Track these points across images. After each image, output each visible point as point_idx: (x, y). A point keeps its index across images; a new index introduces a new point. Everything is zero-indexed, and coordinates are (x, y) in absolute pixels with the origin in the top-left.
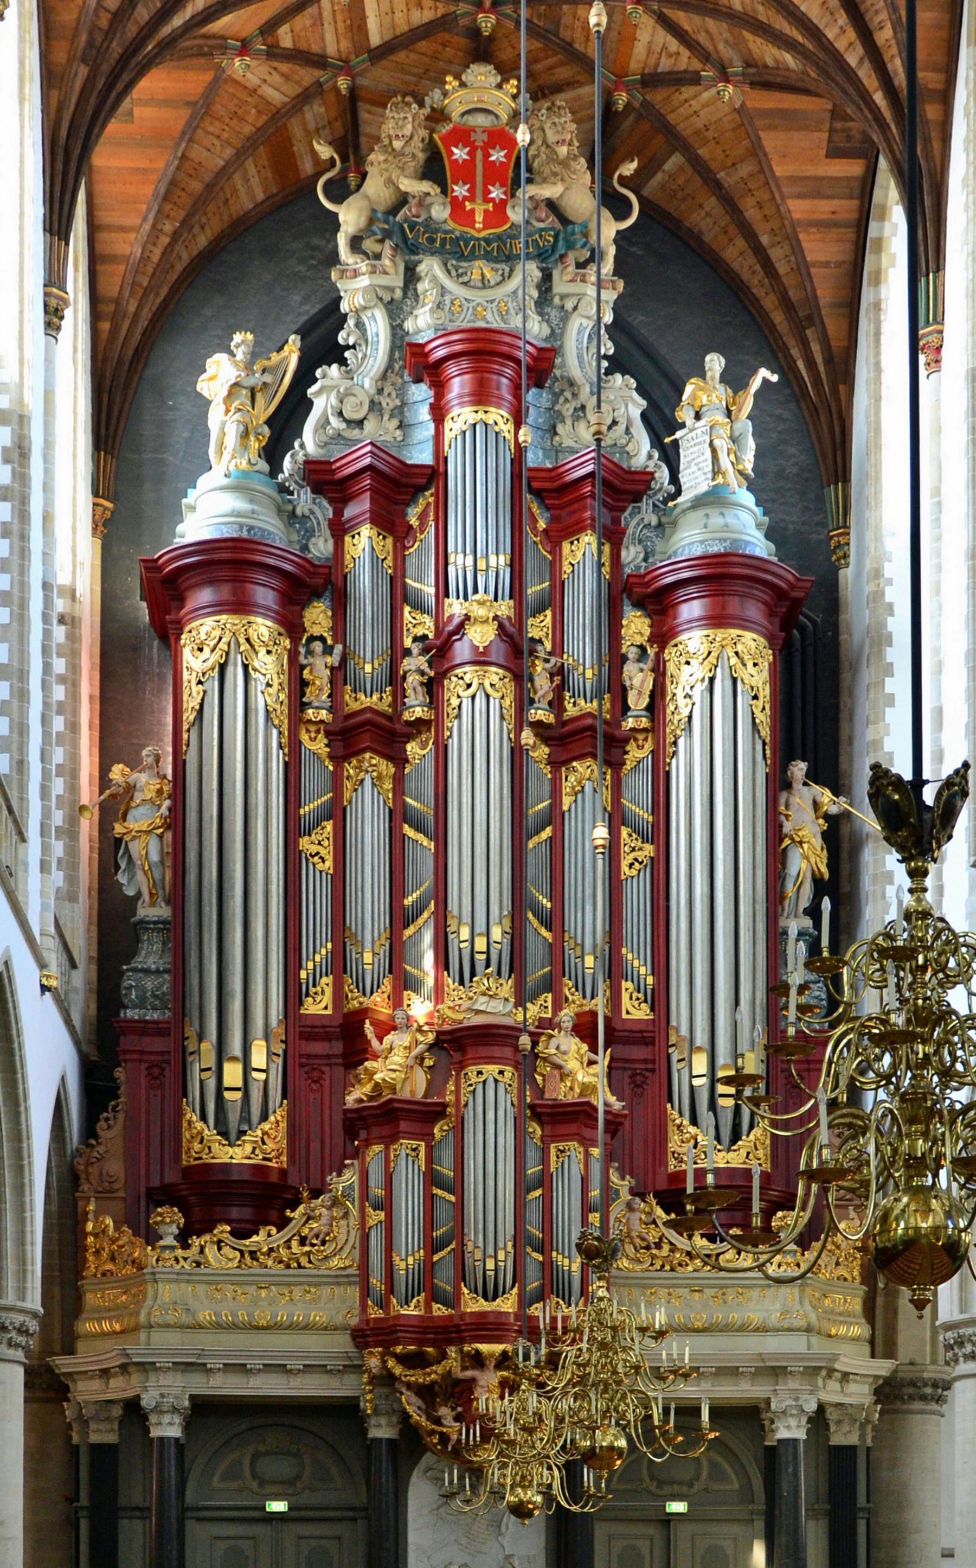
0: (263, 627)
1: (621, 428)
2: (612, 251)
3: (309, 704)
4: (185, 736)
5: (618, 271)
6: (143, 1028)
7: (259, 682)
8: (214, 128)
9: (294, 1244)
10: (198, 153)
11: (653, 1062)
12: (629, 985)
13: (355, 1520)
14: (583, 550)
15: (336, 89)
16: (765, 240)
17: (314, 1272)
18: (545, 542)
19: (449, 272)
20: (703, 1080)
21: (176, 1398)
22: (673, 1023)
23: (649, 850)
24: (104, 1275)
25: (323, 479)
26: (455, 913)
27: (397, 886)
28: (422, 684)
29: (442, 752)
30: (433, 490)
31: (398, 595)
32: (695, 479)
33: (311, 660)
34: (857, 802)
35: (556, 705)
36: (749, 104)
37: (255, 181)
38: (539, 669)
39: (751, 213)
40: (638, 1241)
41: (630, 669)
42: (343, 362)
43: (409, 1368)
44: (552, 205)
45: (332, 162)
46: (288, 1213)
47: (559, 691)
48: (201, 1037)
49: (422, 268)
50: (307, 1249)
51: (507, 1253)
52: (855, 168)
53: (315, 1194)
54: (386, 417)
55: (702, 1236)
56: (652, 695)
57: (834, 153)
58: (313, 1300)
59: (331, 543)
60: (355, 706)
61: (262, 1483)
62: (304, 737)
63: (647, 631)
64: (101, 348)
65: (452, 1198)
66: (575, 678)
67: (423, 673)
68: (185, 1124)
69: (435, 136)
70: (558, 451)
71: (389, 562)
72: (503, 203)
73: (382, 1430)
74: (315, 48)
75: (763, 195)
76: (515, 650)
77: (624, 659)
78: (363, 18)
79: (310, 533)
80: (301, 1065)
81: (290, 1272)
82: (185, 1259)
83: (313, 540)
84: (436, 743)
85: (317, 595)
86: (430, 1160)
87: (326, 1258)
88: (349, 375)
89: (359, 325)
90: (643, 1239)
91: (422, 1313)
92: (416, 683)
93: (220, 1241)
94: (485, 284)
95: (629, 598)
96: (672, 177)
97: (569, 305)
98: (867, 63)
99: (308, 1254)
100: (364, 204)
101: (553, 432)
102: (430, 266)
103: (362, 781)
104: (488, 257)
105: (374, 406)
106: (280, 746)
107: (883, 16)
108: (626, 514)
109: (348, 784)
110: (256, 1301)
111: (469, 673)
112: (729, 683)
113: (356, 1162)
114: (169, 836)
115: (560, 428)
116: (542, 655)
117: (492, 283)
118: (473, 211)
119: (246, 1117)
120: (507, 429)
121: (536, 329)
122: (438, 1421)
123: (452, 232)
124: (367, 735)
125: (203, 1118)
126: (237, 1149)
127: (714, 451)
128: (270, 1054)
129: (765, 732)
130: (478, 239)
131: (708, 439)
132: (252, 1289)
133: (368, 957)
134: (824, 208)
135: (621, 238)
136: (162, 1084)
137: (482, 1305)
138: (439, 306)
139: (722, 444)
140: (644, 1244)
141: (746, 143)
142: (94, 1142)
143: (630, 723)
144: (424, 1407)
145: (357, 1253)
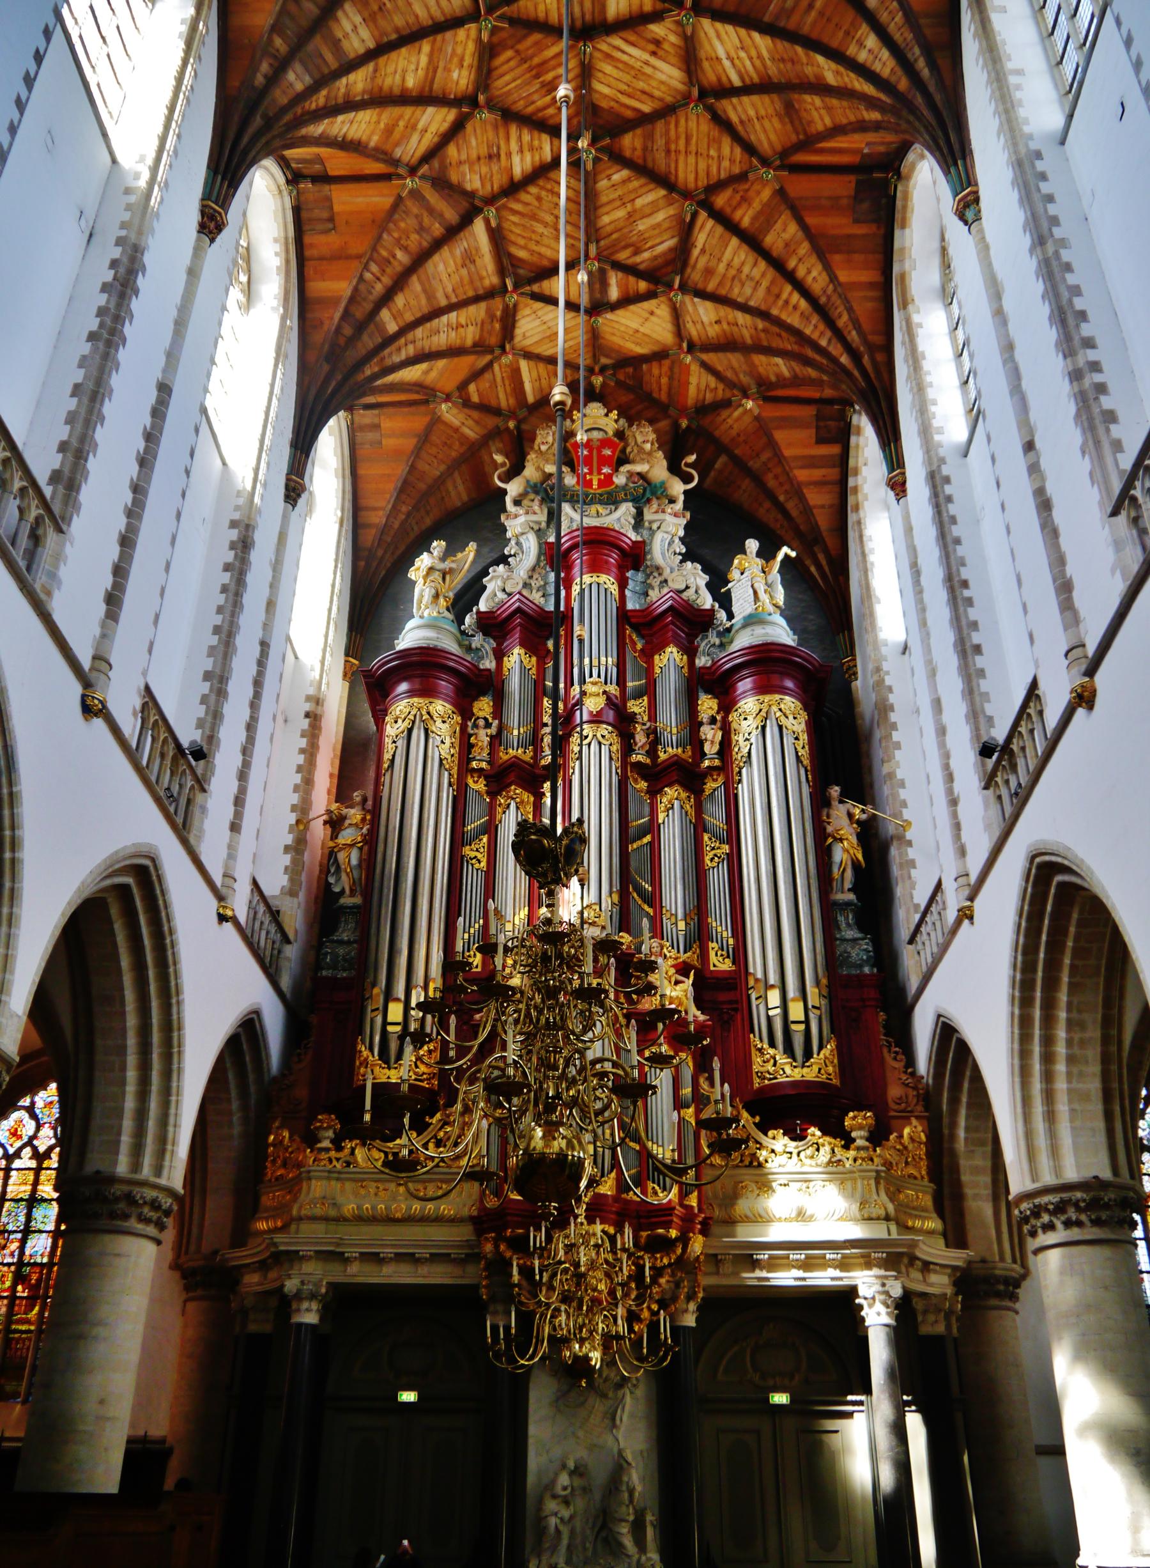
0: (440, 707)
2: (682, 498)
3: (474, 759)
5: (686, 508)
6: (334, 982)
7: (434, 740)
9: (431, 1145)
10: (422, 466)
12: (714, 945)
15: (508, 428)
20: (778, 1011)
21: (315, 1285)
22: (751, 970)
23: (726, 848)
25: (492, 625)
31: (539, 690)
32: (742, 605)
35: (652, 752)
36: (764, 414)
37: (461, 488)
44: (641, 476)
45: (503, 464)
48: (374, 984)
52: (835, 450)
56: (721, 743)
57: (820, 441)
60: (505, 757)
62: (470, 781)
63: (716, 707)
71: (534, 671)
74: (494, 403)
75: (778, 470)
77: (701, 724)
78: (522, 383)
82: (338, 1160)
84: (564, 780)
89: (518, 543)
94: (598, 515)
97: (655, 526)
98: (834, 341)
102: (566, 508)
104: (601, 503)
106: (450, 784)
107: (841, 309)
109: (500, 810)
110: (394, 1198)
111: (587, 729)
112: (776, 729)
115: (650, 592)
121: (633, 536)
125: (371, 1049)
126: (393, 1072)
127: (755, 593)
129: (806, 762)
134: (817, 474)
135: (686, 492)
139: (761, 587)
141: (764, 439)
143: (707, 763)
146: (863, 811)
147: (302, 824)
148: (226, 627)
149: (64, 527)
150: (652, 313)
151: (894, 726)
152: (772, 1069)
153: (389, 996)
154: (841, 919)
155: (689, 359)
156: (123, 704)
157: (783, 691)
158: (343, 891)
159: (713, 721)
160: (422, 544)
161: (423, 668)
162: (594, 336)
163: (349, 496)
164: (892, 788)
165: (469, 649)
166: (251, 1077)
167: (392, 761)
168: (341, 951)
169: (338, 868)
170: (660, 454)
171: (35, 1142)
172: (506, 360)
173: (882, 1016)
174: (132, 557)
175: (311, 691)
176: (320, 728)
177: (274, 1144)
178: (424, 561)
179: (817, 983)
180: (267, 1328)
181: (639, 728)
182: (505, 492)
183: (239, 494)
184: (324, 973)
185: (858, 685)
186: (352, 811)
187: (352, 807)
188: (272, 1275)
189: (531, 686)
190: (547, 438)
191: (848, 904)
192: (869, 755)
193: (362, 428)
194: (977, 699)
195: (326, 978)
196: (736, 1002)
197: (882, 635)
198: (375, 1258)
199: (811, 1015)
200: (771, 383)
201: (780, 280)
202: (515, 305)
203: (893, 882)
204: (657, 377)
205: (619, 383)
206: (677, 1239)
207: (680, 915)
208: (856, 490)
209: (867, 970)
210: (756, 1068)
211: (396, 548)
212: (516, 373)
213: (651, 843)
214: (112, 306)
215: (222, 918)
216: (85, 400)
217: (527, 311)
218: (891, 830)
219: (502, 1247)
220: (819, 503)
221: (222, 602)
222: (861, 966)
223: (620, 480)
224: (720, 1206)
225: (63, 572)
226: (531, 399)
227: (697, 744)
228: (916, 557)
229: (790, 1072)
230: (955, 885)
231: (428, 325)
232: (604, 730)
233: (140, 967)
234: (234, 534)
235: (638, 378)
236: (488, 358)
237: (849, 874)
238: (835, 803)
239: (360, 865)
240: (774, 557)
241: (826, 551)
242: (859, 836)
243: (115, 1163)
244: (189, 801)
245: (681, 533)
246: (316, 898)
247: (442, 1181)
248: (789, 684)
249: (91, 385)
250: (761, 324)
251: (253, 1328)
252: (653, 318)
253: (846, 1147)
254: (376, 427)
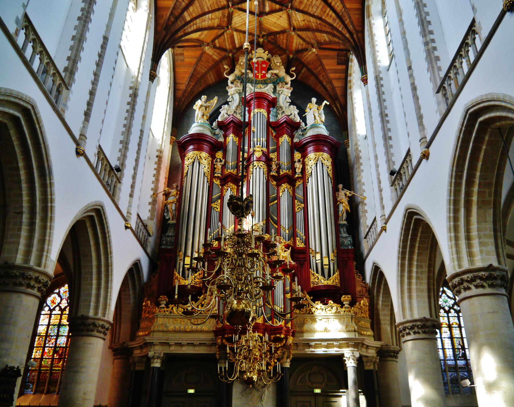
0: (204, 154)
2: (290, 83)
3: (216, 173)
5: (291, 86)
8: (203, 63)
9: (200, 306)
10: (199, 69)
12: (298, 238)
16: (325, 84)
22: (311, 247)
23: (303, 205)
32: (310, 121)
36: (319, 54)
39: (321, 78)
44: (276, 74)
48: (180, 251)
52: (344, 67)
56: (302, 169)
57: (339, 64)
60: (227, 173)
62: (214, 181)
63: (300, 156)
71: (237, 142)
74: (224, 47)
75: (323, 74)
77: (295, 162)
78: (234, 40)
84: (247, 181)
89: (232, 97)
94: (261, 88)
96: (303, 74)
97: (280, 92)
101: (277, 116)
102: (249, 85)
104: (262, 84)
105: (235, 112)
106: (207, 182)
109: (225, 191)
110: (187, 324)
111: (255, 163)
112: (321, 164)
114: (178, 203)
120: (266, 114)
121: (273, 96)
125: (179, 273)
126: (187, 281)
127: (315, 117)
129: (331, 176)
134: (337, 75)
135: (291, 81)
141: (319, 63)
143: (297, 176)
146: (350, 193)
147: (155, 195)
148: (128, 125)
149: (69, 88)
150: (281, 17)
151: (361, 164)
152: (317, 281)
153: (185, 255)
154: (342, 230)
155: (293, 33)
156: (91, 152)
157: (323, 151)
158: (169, 219)
159: (299, 161)
160: (198, 97)
161: (198, 141)
162: (260, 24)
163: (172, 79)
164: (360, 185)
165: (214, 134)
166: (137, 283)
167: (187, 173)
168: (169, 239)
169: (168, 210)
170: (283, 67)
171: (60, 305)
172: (228, 32)
173: (355, 263)
174: (94, 99)
175: (159, 148)
176: (162, 161)
177: (145, 306)
178: (199, 103)
179: (333, 252)
180: (143, 368)
181: (273, 163)
182: (228, 79)
183: (133, 77)
184: (163, 247)
185: (349, 149)
186: (173, 191)
187: (173, 189)
188: (144, 350)
189: (236, 148)
190: (243, 60)
191: (344, 225)
192: (352, 174)
193: (177, 55)
194: (390, 155)
195: (163, 248)
196: (305, 258)
197: (358, 133)
198: (180, 345)
199: (331, 263)
200: (322, 43)
201: (325, 5)
202: (232, 12)
203: (360, 217)
204: (282, 39)
205: (268, 41)
206: (284, 338)
207: (287, 228)
208: (350, 81)
209: (350, 247)
210: (311, 280)
211: (189, 98)
212: (232, 37)
213: (277, 203)
214: (86, 7)
215: (127, 228)
216: (77, 42)
217: (236, 14)
218: (360, 200)
219: (224, 341)
220: (338, 86)
221: (127, 116)
222: (348, 246)
223: (268, 76)
224: (298, 327)
225: (69, 104)
226: (237, 46)
227: (294, 169)
228: (370, 105)
229: (323, 282)
230: (380, 219)
231: (201, 18)
232: (261, 163)
233: (97, 244)
234: (131, 92)
235: (276, 40)
236: (223, 31)
237: (345, 215)
238: (340, 190)
239: (175, 210)
240: (322, 104)
241: (340, 103)
242: (348, 202)
243: (89, 312)
244: (115, 186)
245: (290, 95)
246: (160, 221)
247: (204, 318)
248: (326, 149)
249: (79, 36)
250: (319, 22)
251: (137, 368)
252: (281, 18)
253: (342, 307)
254: (182, 54)
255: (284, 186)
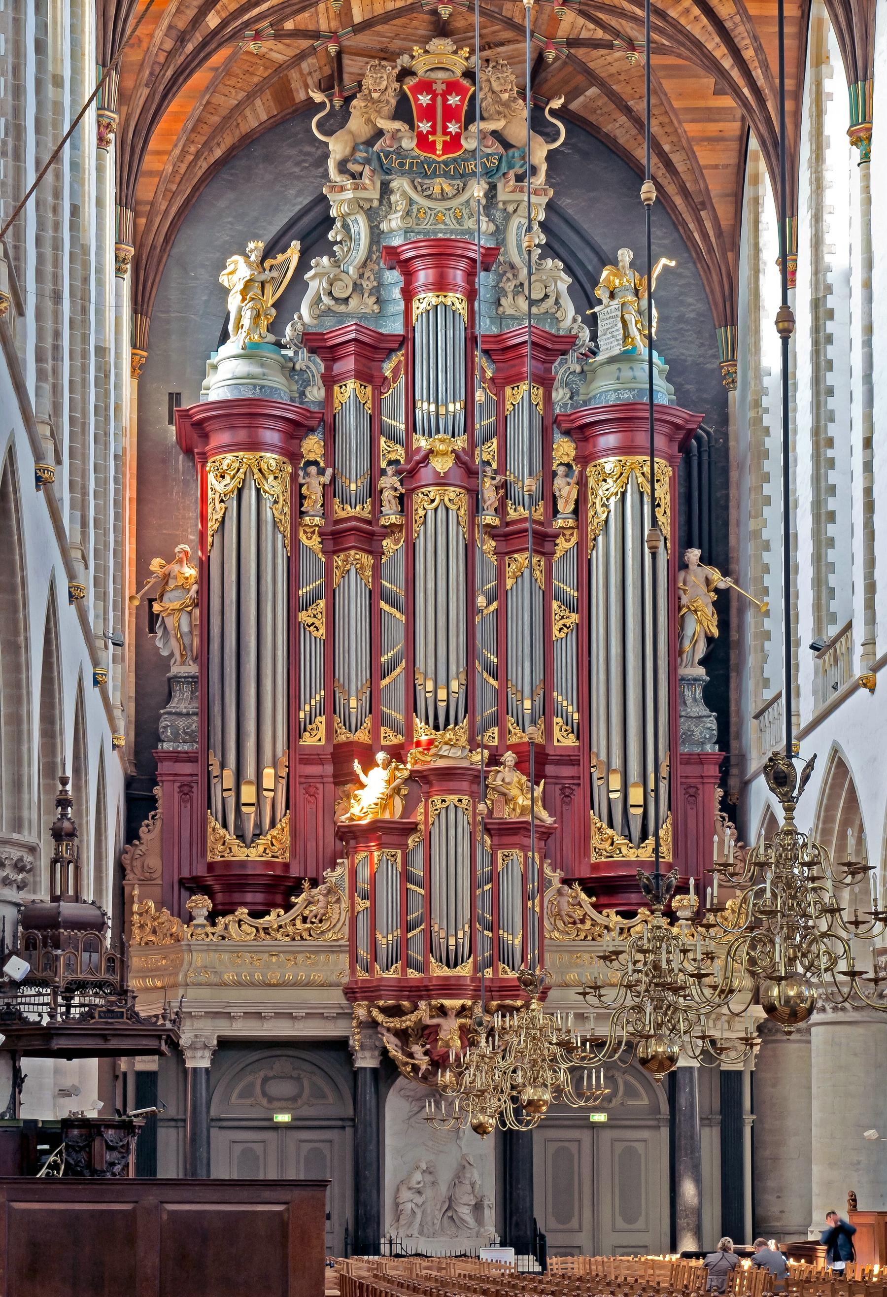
1: (551, 301)
4: (210, 539)
11: (579, 778)
13: (343, 1128)
14: (521, 395)
17: (314, 943)
18: (492, 387)
19: (415, 188)
21: (207, 1038)
24: (147, 944)
26: (422, 669)
27: (375, 647)
28: (395, 497)
29: (411, 549)
30: (403, 352)
33: (308, 480)
34: (741, 581)
38: (487, 485)
40: (566, 919)
41: (559, 482)
42: (332, 254)
43: (390, 1016)
44: (495, 134)
46: (293, 899)
47: (503, 501)
49: (394, 185)
50: (308, 925)
51: (464, 932)
53: (314, 883)
54: (366, 295)
55: (617, 913)
56: (577, 502)
58: (313, 964)
59: (323, 392)
60: (342, 514)
61: (271, 1100)
63: (573, 453)
64: (139, 237)
65: (422, 892)
66: (516, 489)
67: (396, 490)
68: (210, 830)
69: (405, 87)
70: (501, 318)
71: (369, 405)
72: (458, 135)
73: (366, 1061)
76: (468, 471)
77: (554, 474)
79: (307, 383)
80: (300, 783)
81: (295, 943)
82: (213, 934)
83: (309, 388)
85: (312, 430)
86: (405, 863)
87: (323, 932)
88: (337, 264)
89: (346, 226)
90: (570, 917)
91: (399, 976)
92: (390, 497)
93: (240, 921)
95: (558, 428)
97: (510, 209)
99: (309, 930)
100: (348, 137)
103: (348, 571)
104: (446, 175)
105: (357, 287)
108: (556, 364)
113: (346, 861)
115: (503, 301)
116: (490, 474)
117: (450, 195)
118: (434, 142)
119: (259, 825)
122: (411, 1055)
123: (418, 157)
124: (352, 537)
128: (277, 777)
130: (438, 163)
131: (619, 314)
132: (265, 956)
133: (353, 703)
136: (191, 799)
137: (445, 971)
138: (408, 213)
140: (571, 920)
142: (137, 842)
143: (560, 523)
144: (399, 1044)
145: (346, 929)
181: (488, 483)
253: (672, 924)
255: (521, 558)
